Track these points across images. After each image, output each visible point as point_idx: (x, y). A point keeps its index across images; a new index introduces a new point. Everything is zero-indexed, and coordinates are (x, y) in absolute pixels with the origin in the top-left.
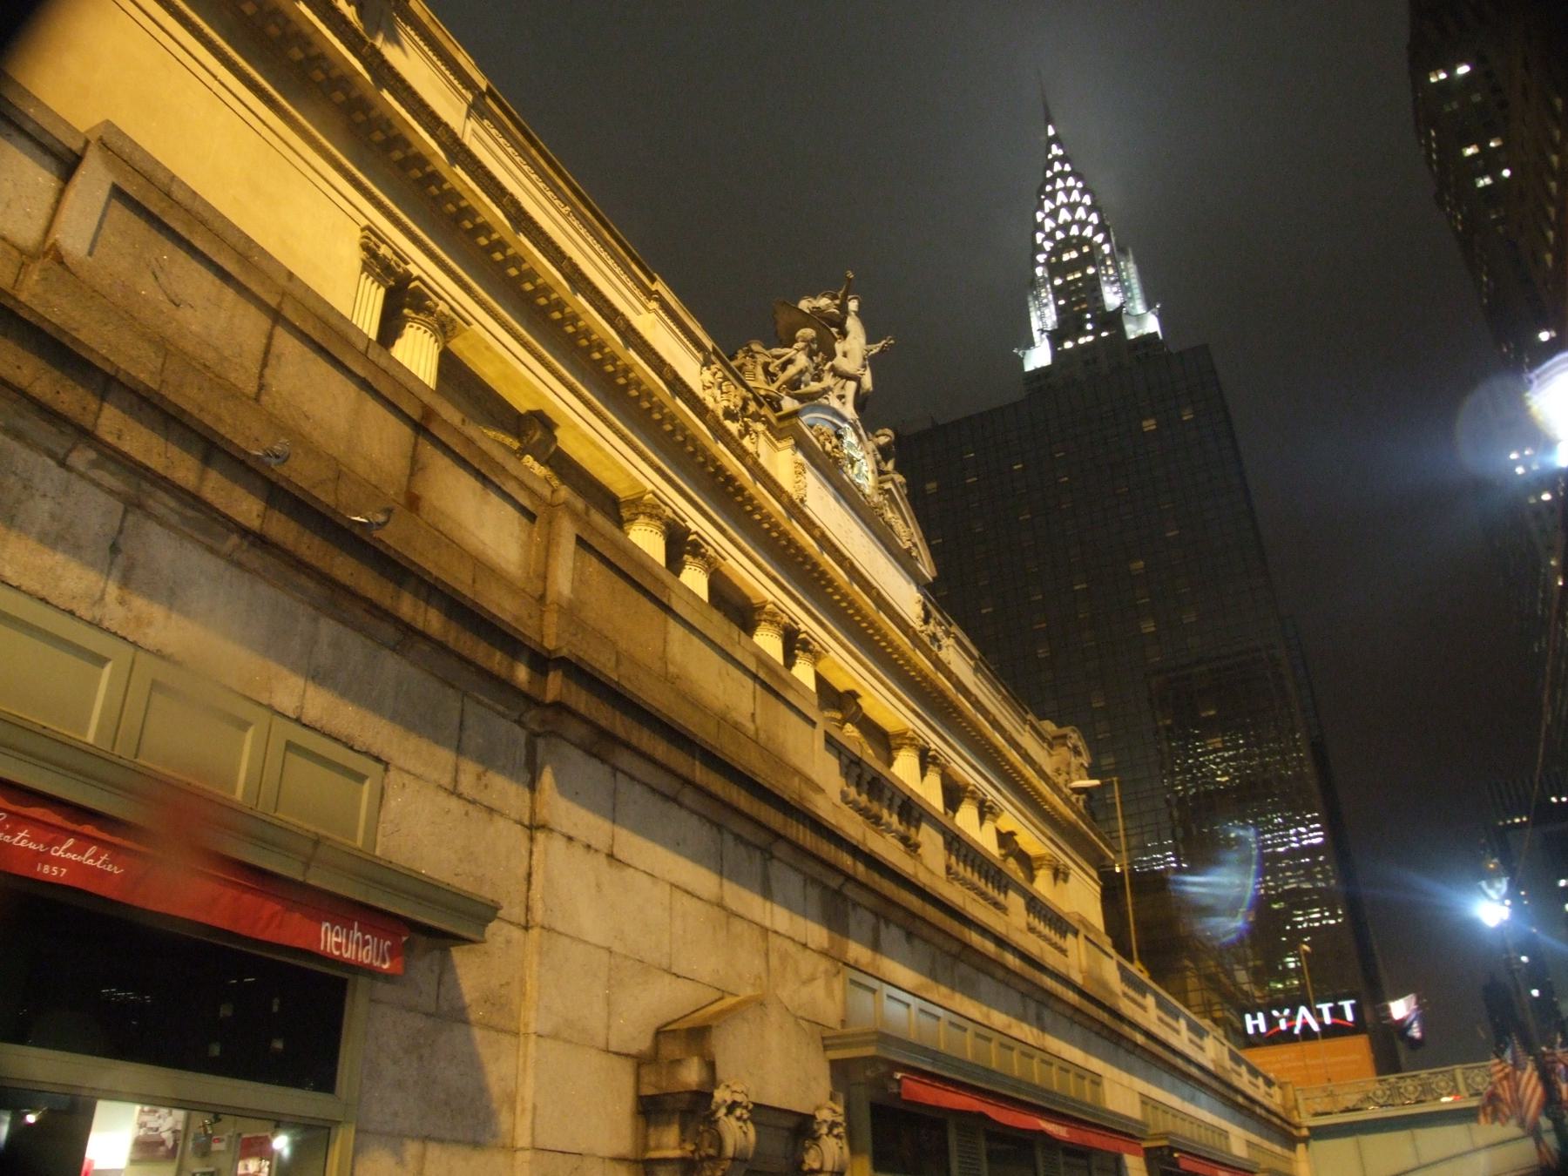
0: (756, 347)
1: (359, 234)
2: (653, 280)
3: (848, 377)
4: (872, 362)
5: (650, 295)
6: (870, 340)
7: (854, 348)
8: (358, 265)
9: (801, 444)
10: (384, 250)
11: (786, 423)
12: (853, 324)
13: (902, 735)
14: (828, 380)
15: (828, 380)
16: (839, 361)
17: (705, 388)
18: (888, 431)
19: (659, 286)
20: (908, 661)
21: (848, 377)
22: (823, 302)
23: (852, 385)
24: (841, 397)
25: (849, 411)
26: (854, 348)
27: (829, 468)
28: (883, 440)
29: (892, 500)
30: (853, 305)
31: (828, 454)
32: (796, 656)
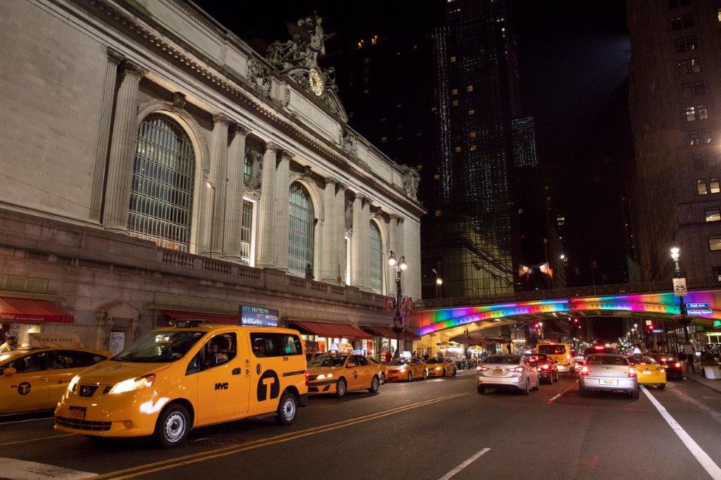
0: (277, 43)
1: (106, 49)
2: (226, 32)
3: (314, 50)
4: (327, 43)
5: (225, 38)
6: (325, 33)
8: (106, 59)
9: (288, 82)
10: (116, 54)
11: (284, 75)
12: (318, 29)
13: (329, 178)
14: (308, 51)
15: (308, 51)
16: (313, 45)
17: (249, 68)
18: (333, 68)
19: (230, 35)
20: (332, 154)
21: (315, 51)
22: (308, 20)
23: (316, 54)
24: (312, 58)
25: (314, 64)
26: (317, 40)
27: (303, 89)
28: (331, 71)
29: (331, 95)
30: (319, 21)
31: (300, 85)
32: (282, 158)
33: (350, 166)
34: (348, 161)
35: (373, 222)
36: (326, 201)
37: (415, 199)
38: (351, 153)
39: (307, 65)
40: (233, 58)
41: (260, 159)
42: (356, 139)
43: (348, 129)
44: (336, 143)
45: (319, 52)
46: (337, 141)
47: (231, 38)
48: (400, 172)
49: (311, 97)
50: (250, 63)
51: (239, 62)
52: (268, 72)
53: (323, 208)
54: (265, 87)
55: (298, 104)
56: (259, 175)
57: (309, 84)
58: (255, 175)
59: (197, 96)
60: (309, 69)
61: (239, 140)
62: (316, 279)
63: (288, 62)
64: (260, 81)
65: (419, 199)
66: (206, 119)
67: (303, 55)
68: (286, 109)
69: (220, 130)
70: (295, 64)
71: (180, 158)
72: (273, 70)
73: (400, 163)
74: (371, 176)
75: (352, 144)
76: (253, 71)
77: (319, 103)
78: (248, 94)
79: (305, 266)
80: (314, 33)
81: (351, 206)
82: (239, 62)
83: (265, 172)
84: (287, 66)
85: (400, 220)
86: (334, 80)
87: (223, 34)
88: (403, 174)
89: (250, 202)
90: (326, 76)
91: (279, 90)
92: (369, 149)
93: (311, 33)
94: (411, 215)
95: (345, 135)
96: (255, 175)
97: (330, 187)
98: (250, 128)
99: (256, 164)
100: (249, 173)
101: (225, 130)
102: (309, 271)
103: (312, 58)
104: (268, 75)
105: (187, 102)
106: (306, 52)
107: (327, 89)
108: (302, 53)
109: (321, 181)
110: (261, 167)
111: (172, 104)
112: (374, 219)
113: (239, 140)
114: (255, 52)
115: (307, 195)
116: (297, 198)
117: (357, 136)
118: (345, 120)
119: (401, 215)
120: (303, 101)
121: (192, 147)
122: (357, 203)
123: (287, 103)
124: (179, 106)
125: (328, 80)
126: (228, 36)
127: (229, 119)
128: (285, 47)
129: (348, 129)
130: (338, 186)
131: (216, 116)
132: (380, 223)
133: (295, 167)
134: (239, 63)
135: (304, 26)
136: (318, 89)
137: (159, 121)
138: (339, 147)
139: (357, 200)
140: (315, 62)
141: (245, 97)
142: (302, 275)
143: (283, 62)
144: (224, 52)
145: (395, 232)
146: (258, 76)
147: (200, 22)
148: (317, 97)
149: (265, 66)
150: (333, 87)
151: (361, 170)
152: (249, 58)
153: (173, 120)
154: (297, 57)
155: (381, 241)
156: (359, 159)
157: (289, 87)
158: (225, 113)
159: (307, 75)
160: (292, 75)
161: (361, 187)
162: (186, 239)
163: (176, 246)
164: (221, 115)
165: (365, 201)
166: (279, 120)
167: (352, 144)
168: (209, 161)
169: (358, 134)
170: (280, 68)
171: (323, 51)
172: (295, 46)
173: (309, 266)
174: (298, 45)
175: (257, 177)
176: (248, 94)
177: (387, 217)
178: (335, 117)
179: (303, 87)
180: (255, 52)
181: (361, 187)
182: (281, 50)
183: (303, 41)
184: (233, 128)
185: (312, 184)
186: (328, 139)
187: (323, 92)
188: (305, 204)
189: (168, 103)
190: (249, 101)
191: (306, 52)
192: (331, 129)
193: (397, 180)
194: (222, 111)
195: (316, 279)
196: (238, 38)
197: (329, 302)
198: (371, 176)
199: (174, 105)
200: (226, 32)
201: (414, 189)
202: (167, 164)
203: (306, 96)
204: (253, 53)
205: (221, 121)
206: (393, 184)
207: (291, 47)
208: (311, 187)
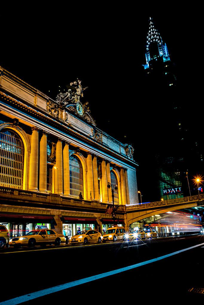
5: (36, 93)
6: (83, 87)
7: (79, 91)
14: (76, 96)
18: (87, 102)
19: (38, 92)
22: (75, 82)
23: (79, 97)
27: (74, 113)
28: (87, 104)
29: (87, 114)
30: (80, 83)
35: (111, 171)
36: (88, 164)
37: (132, 159)
38: (99, 140)
39: (75, 103)
40: (40, 102)
41: (55, 146)
42: (101, 134)
43: (97, 129)
44: (91, 136)
45: (81, 96)
46: (92, 135)
47: (39, 93)
48: (124, 147)
49: (77, 116)
50: (48, 103)
51: (43, 103)
52: (57, 107)
53: (87, 166)
54: (56, 114)
55: (71, 120)
56: (55, 153)
57: (76, 110)
58: (52, 153)
59: (23, 119)
60: (76, 104)
61: (44, 137)
62: (85, 199)
63: (65, 101)
64: (53, 111)
65: (134, 159)
66: (28, 130)
67: (73, 98)
68: (66, 123)
69: (35, 133)
70: (70, 102)
71: (17, 147)
72: (59, 105)
73: (124, 143)
76: (49, 107)
79: (79, 193)
80: (78, 88)
81: (101, 164)
82: (43, 103)
83: (57, 151)
84: (66, 103)
85: (125, 170)
86: (88, 108)
88: (126, 148)
90: (85, 106)
92: (108, 138)
93: (77, 88)
94: (131, 167)
95: (95, 132)
96: (52, 153)
97: (89, 156)
99: (53, 148)
100: (50, 152)
101: (38, 133)
102: (81, 196)
103: (78, 99)
104: (57, 108)
105: (20, 123)
106: (74, 96)
107: (85, 112)
108: (73, 97)
109: (85, 154)
110: (55, 149)
111: (12, 124)
112: (113, 170)
113: (44, 137)
114: (50, 99)
116: (75, 163)
117: (102, 132)
118: (94, 124)
119: (126, 167)
120: (74, 118)
121: (23, 142)
122: (103, 163)
124: (16, 124)
125: (86, 108)
127: (39, 129)
128: (65, 95)
129: (97, 129)
130: (93, 156)
131: (33, 128)
132: (116, 172)
133: (71, 148)
134: (43, 105)
135: (73, 85)
136: (81, 112)
137: (7, 132)
138: (92, 138)
140: (79, 101)
142: (78, 197)
143: (64, 101)
145: (123, 175)
146: (52, 108)
148: (80, 116)
150: (88, 111)
152: (48, 101)
153: (14, 131)
154: (70, 99)
155: (117, 180)
156: (103, 143)
157: (67, 112)
158: (37, 126)
159: (75, 107)
160: (68, 107)
162: (20, 183)
163: (16, 187)
164: (35, 127)
165: (107, 162)
167: (99, 136)
168: (30, 148)
170: (62, 104)
171: (82, 96)
172: (69, 94)
173: (81, 193)
174: (70, 93)
175: (54, 154)
177: (119, 168)
178: (90, 124)
180: (50, 99)
182: (63, 96)
183: (73, 92)
184: (41, 133)
186: (87, 134)
187: (84, 114)
189: (11, 123)
191: (74, 96)
192: (88, 131)
193: (123, 151)
194: (36, 125)
195: (85, 199)
196: (42, 93)
199: (13, 124)
200: (36, 91)
201: (131, 155)
202: (11, 151)
205: (36, 130)
206: (121, 153)
207: (67, 95)
208: (81, 157)
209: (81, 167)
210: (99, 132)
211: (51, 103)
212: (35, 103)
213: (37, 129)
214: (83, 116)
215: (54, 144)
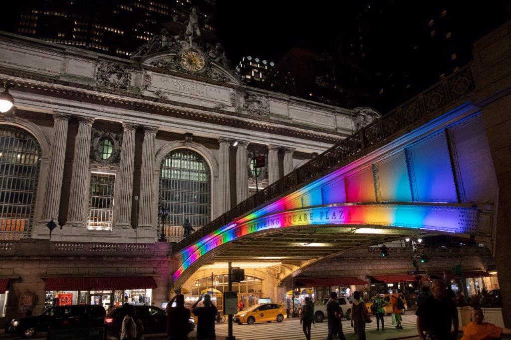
5: (66, 54)
9: (147, 69)
14: (186, 38)
31: (162, 67)
33: (247, 123)
34: (240, 118)
42: (267, 97)
48: (349, 115)
50: (99, 65)
52: (121, 67)
74: (283, 126)
75: (259, 102)
77: (203, 77)
78: (79, 90)
87: (62, 51)
89: (111, 176)
91: (135, 78)
98: (93, 116)
103: (189, 42)
115: (200, 159)
117: (268, 94)
120: (171, 80)
123: (146, 86)
126: (67, 51)
138: (233, 110)
139: (270, 151)
141: (80, 94)
144: (64, 65)
146: (111, 73)
147: (33, 49)
149: (117, 64)
151: (267, 124)
157: (149, 73)
160: (152, 63)
161: (271, 138)
166: (130, 102)
167: (259, 102)
169: (268, 92)
176: (79, 90)
178: (222, 83)
179: (165, 68)
181: (271, 138)
185: (199, 148)
188: (195, 165)
190: (86, 95)
192: (219, 96)
197: (45, 258)
198: (283, 126)
203: (175, 75)
204: (100, 57)
208: (201, 150)
209: (208, 171)
210: (261, 96)
211: (109, 63)
212: (64, 70)
213: (62, 117)
214: (204, 71)
215: (115, 135)
